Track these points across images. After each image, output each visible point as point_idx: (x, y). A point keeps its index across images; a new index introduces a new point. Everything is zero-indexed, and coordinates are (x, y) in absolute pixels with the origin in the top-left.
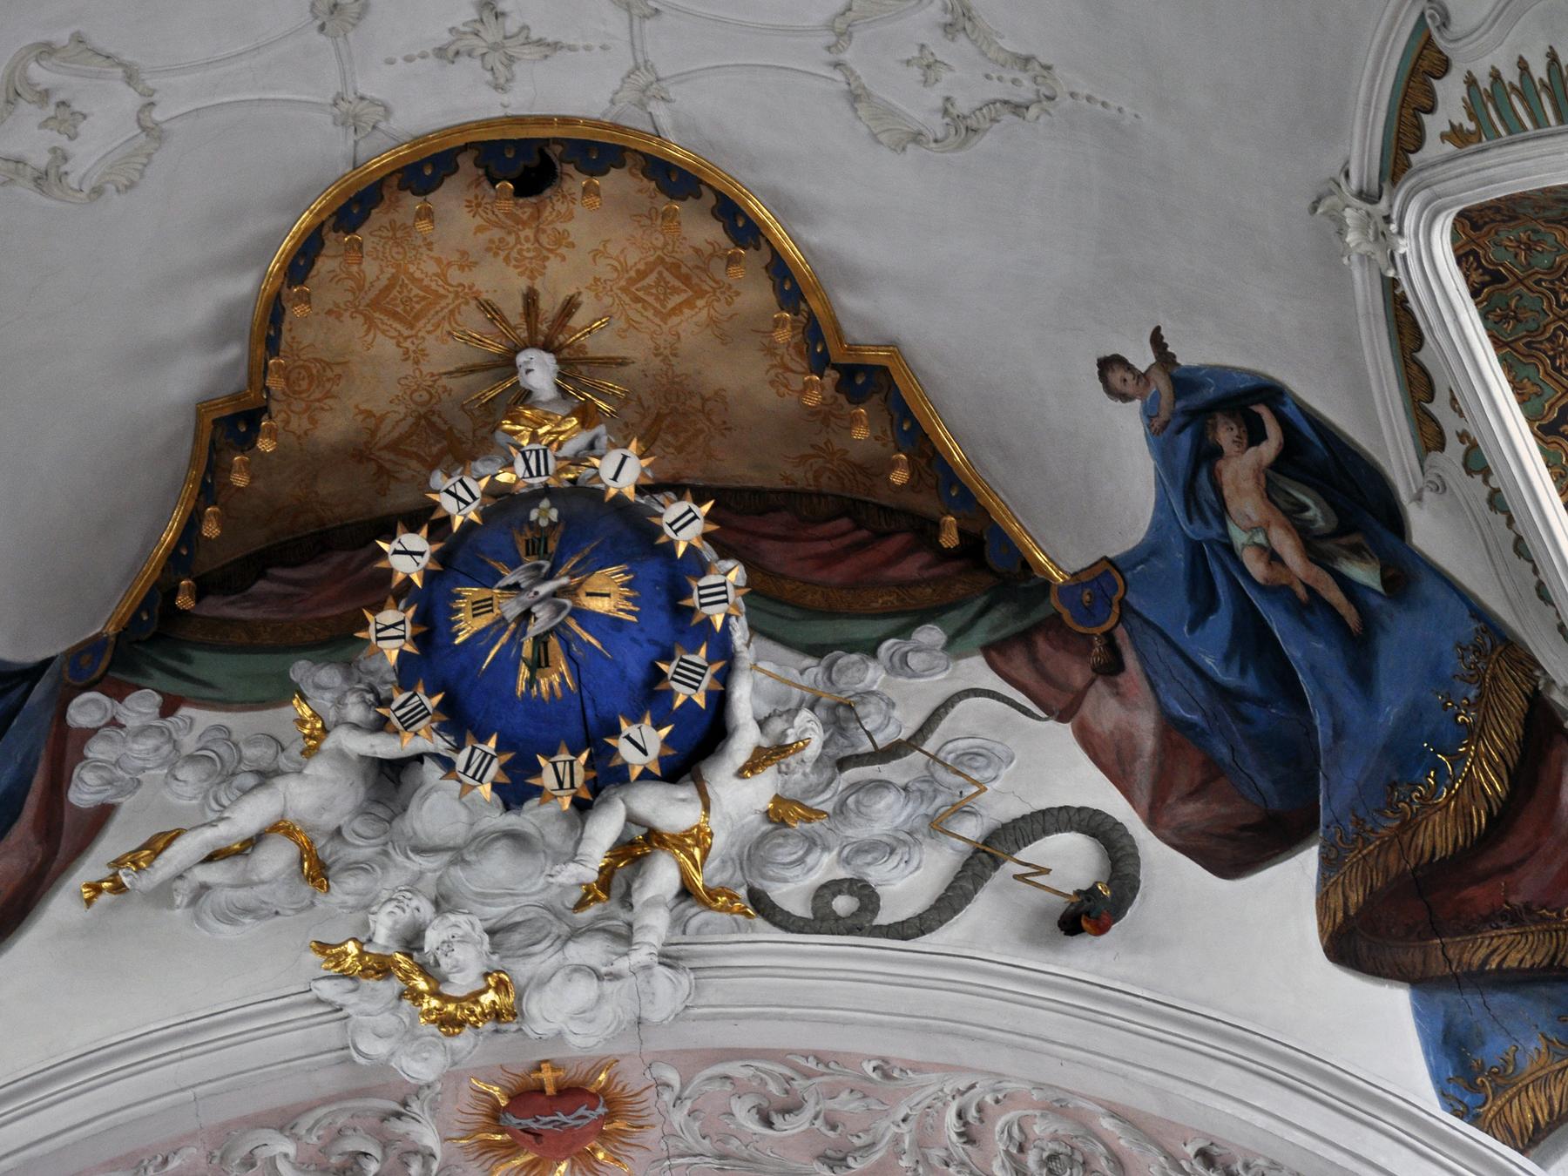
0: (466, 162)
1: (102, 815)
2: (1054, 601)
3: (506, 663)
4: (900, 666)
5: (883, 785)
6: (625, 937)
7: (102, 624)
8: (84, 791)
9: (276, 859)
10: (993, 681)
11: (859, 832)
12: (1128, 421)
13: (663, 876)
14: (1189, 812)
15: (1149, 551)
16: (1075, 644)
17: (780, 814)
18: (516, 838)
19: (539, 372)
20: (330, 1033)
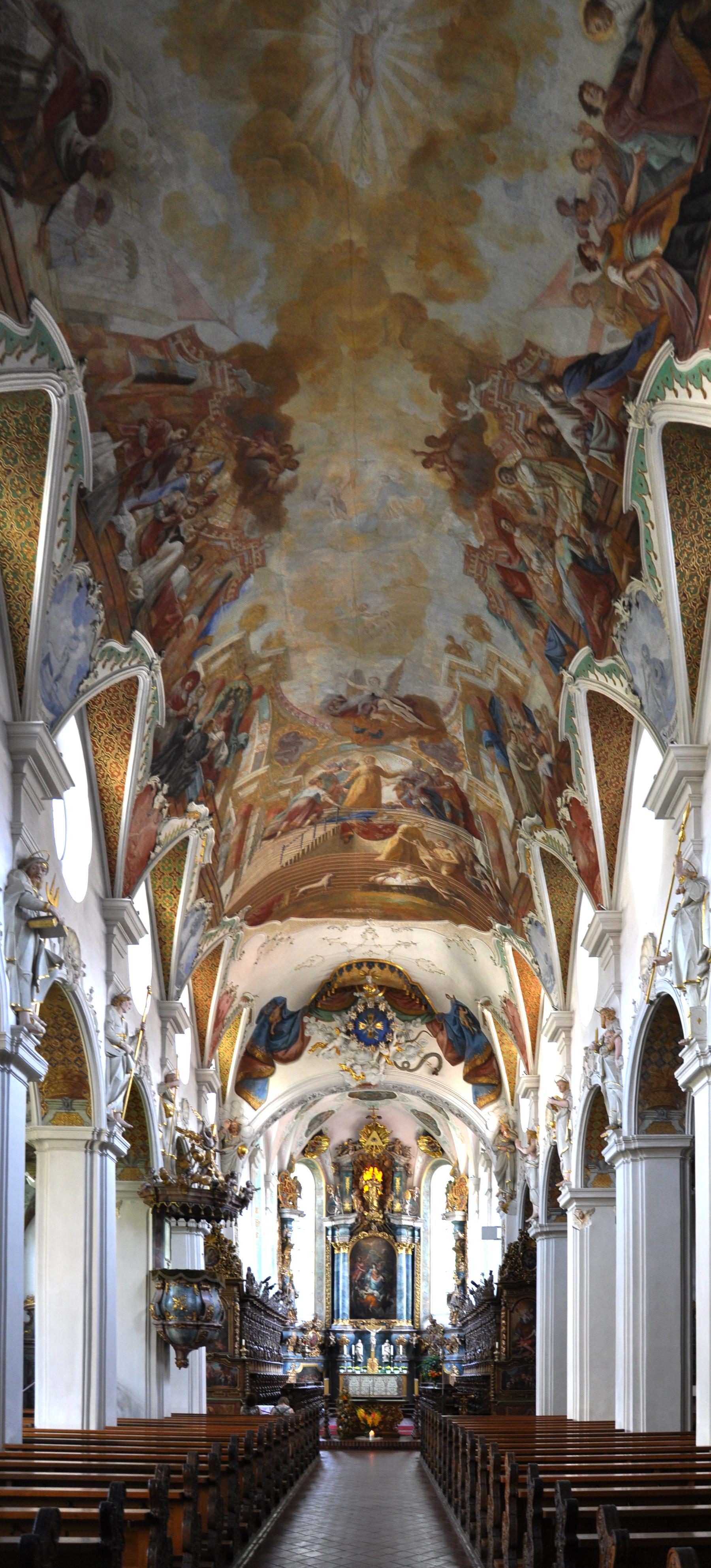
0: (365, 964)
1: (309, 1038)
2: (436, 1017)
3: (366, 1034)
4: (415, 1026)
5: (411, 1046)
6: (378, 1068)
7: (307, 1004)
8: (307, 1034)
9: (334, 1051)
10: (426, 1029)
11: (408, 1054)
12: (449, 1001)
13: (383, 1060)
14: (449, 1055)
15: (449, 1015)
16: (438, 1024)
17: (398, 1051)
18: (364, 1051)
19: (369, 979)
20: (341, 1078)
